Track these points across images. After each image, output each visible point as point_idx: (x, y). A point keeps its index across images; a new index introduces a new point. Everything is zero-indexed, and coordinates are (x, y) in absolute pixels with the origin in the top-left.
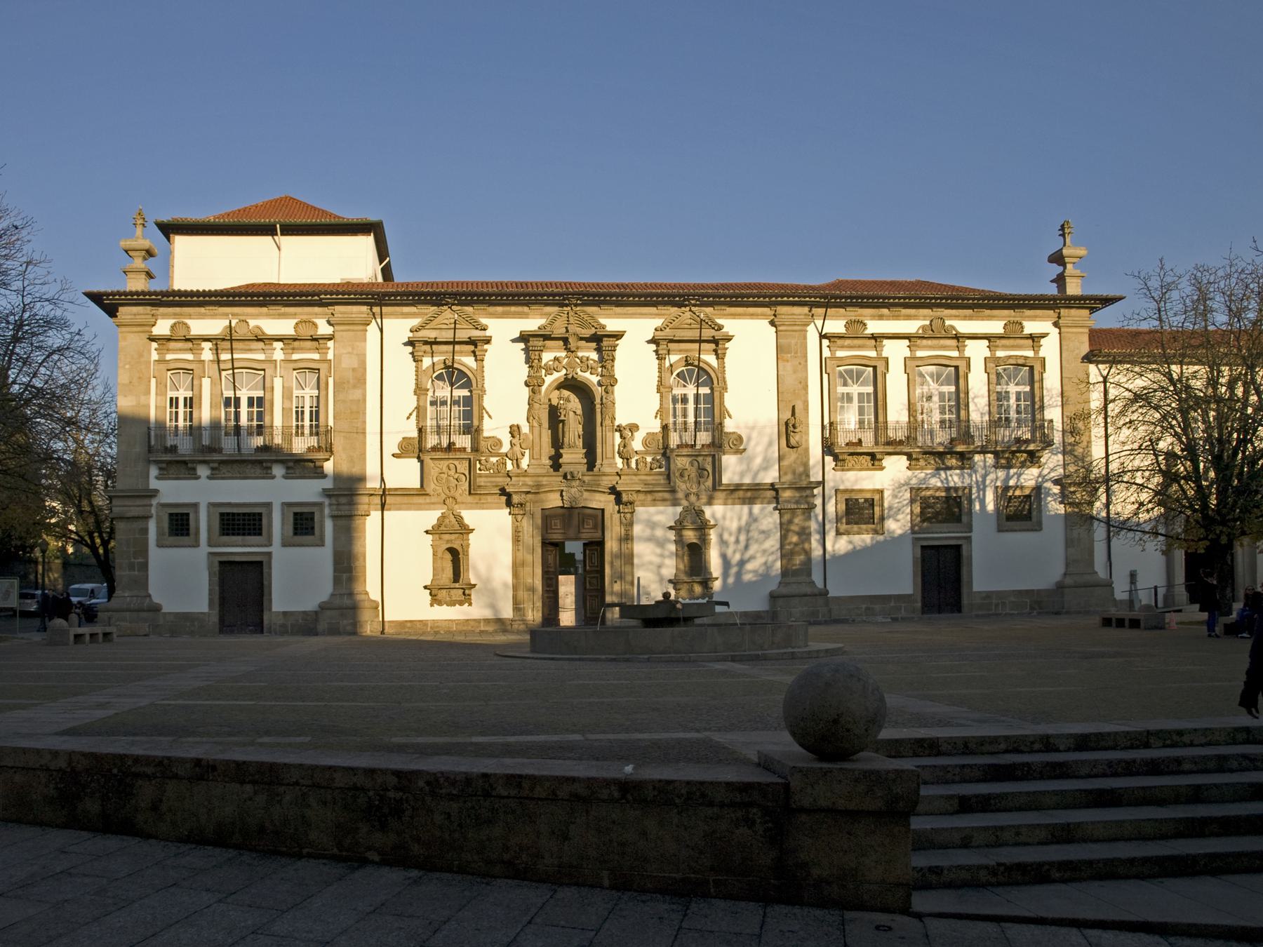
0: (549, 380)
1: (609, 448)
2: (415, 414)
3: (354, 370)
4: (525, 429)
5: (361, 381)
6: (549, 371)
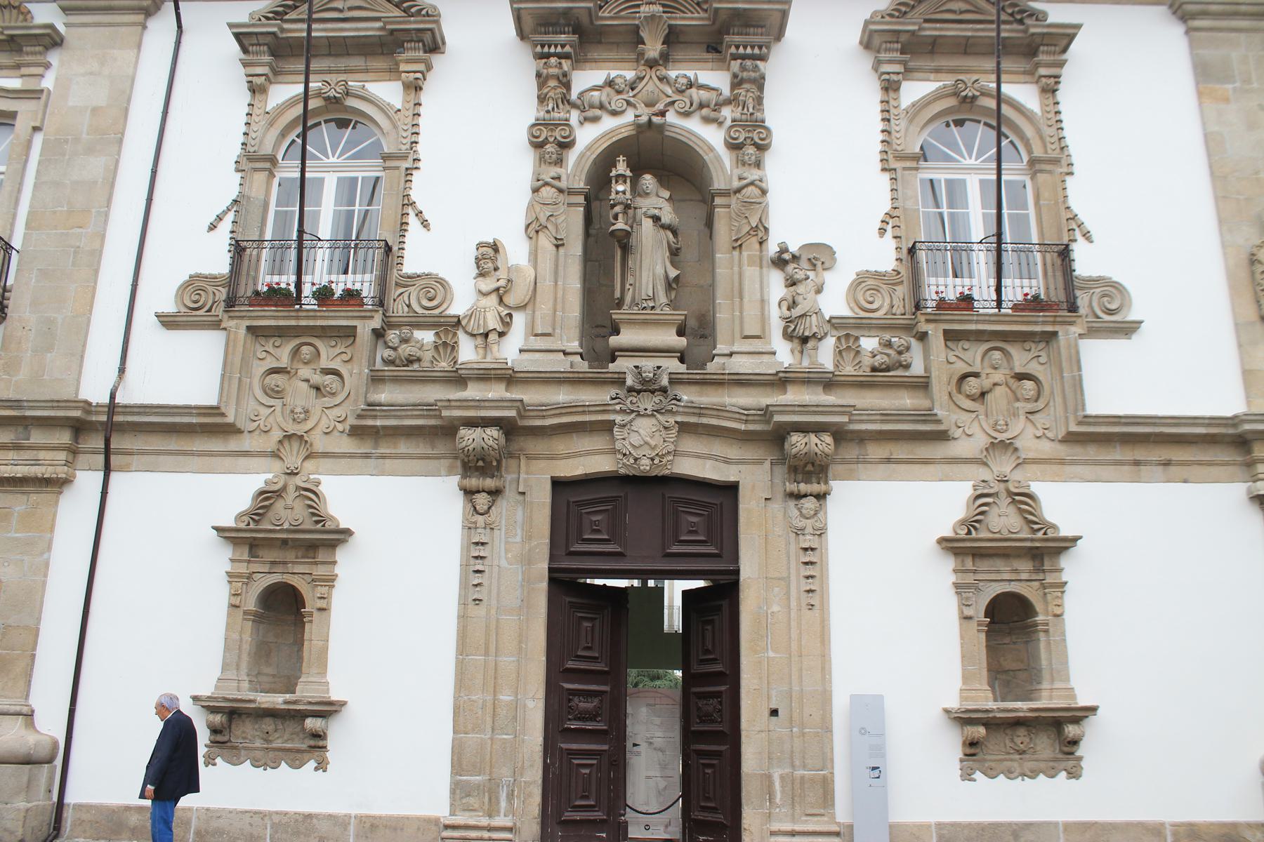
0: (589, 137)
1: (751, 310)
2: (230, 216)
3: (95, 110)
4: (517, 252)
5: (111, 136)
6: (591, 111)
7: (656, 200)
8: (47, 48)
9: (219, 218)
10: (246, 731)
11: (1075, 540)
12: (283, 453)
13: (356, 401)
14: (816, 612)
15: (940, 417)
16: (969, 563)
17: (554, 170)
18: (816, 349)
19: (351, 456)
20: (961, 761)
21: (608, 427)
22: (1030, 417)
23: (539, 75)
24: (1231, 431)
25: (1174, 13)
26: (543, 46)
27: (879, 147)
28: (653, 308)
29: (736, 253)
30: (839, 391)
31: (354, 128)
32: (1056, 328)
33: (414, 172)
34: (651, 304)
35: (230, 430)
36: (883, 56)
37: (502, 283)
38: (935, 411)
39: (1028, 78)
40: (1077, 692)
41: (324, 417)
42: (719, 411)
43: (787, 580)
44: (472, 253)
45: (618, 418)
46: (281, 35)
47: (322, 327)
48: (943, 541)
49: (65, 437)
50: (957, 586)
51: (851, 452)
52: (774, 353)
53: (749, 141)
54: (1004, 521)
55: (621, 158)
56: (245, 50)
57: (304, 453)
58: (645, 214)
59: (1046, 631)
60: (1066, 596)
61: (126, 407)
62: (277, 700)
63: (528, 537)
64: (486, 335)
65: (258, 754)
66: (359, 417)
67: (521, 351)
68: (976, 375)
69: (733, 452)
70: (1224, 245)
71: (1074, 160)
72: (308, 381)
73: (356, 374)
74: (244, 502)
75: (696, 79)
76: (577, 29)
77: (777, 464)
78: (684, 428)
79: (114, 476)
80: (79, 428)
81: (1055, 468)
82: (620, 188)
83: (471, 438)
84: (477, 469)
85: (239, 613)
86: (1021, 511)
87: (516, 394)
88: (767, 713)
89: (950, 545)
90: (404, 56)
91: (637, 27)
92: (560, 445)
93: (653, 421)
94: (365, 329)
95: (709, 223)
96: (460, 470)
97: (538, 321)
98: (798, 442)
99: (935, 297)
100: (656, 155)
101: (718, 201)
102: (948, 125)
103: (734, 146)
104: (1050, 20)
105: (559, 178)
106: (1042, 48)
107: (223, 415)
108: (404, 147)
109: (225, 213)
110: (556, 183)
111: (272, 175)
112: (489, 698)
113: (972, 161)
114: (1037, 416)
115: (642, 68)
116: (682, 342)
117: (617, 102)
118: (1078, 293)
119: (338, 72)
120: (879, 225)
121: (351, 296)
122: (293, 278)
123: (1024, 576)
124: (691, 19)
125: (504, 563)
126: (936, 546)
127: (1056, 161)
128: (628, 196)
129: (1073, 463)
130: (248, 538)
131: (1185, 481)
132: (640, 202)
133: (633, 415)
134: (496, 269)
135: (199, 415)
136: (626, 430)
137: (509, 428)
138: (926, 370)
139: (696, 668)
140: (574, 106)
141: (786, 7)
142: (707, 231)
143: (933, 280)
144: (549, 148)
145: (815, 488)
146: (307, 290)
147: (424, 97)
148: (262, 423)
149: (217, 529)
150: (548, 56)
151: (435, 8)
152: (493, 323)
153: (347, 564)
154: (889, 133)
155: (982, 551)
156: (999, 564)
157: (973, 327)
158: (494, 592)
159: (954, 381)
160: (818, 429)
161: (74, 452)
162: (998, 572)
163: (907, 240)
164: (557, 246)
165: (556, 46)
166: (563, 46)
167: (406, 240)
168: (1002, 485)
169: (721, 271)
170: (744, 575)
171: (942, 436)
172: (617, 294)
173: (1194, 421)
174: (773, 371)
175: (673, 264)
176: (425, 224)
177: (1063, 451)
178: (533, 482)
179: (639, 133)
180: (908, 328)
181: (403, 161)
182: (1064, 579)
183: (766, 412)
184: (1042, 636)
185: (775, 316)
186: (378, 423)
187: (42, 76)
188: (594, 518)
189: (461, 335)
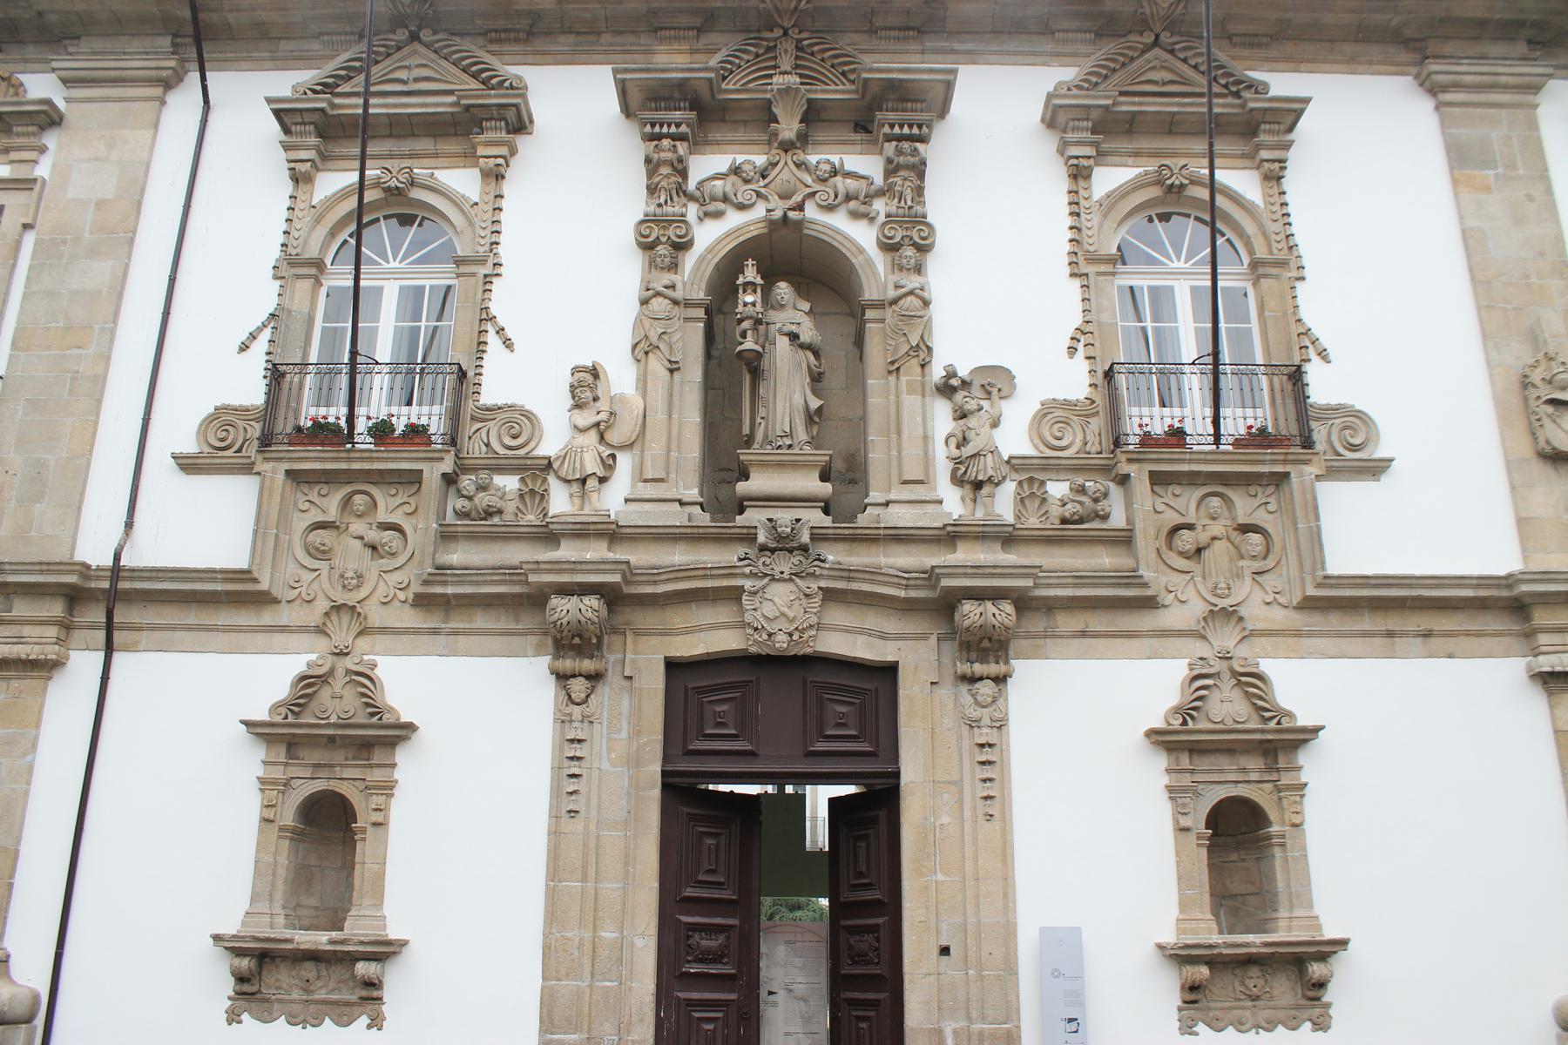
0: (710, 236)
1: (911, 450)
2: (266, 334)
3: (100, 204)
4: (621, 378)
5: (119, 235)
7: (793, 313)
8: (42, 128)
9: (253, 336)
10: (281, 980)
11: (1316, 730)
12: (330, 629)
13: (421, 563)
14: (996, 824)
15: (1146, 579)
16: (1185, 761)
17: (667, 278)
18: (991, 496)
19: (416, 632)
20: (1180, 1009)
21: (735, 595)
22: (1258, 578)
23: (648, 161)
24: (1505, 593)
25: (1421, 85)
26: (653, 125)
27: (1067, 247)
28: (790, 446)
29: (892, 378)
30: (1023, 549)
31: (420, 225)
32: (1288, 468)
33: (494, 280)
34: (788, 442)
35: (264, 599)
36: (1070, 136)
37: (603, 416)
38: (1141, 572)
39: (1247, 163)
40: (1322, 921)
41: (382, 583)
42: (873, 574)
43: (958, 783)
44: (566, 379)
45: (748, 584)
46: (330, 112)
47: (380, 471)
48: (1152, 733)
49: (56, 609)
50: (1170, 789)
51: (1037, 623)
52: (941, 502)
53: (907, 241)
54: (1228, 708)
55: (750, 262)
56: (286, 130)
57: (356, 629)
58: (780, 331)
59: (1283, 845)
60: (1306, 800)
61: (133, 570)
62: (320, 939)
63: (636, 732)
64: (583, 481)
65: (296, 1008)
66: (426, 583)
67: (627, 501)
68: (1190, 527)
69: (892, 625)
70: (1490, 365)
71: (1305, 262)
72: (362, 538)
73: (420, 530)
74: (282, 690)
75: (842, 165)
76: (696, 105)
77: (946, 639)
78: (829, 595)
79: (118, 658)
80: (74, 597)
81: (1290, 640)
82: (749, 299)
83: (565, 609)
84: (572, 647)
85: (275, 828)
86: (1248, 695)
87: (620, 554)
88: (936, 951)
89: (1161, 739)
90: (482, 138)
91: (769, 102)
92: (677, 617)
93: (791, 587)
94: (433, 473)
95: (859, 342)
96: (551, 649)
97: (648, 464)
98: (970, 612)
99: (1138, 431)
100: (793, 259)
101: (869, 314)
102: (1150, 220)
103: (889, 247)
104: (1271, 93)
105: (673, 287)
106: (1263, 127)
107: (255, 580)
108: (482, 249)
109: (260, 329)
110: (669, 292)
111: (318, 283)
112: (588, 935)
113: (1181, 264)
114: (1267, 576)
115: (774, 151)
116: (826, 489)
117: (744, 194)
118: (1313, 424)
119: (402, 157)
120: (1068, 343)
121: (416, 433)
122: (344, 411)
123: (1254, 776)
124: (834, 92)
125: (606, 765)
126: (1145, 742)
127: (1282, 264)
128: (759, 308)
129: (1311, 634)
130: (287, 734)
131: (1450, 656)
132: (773, 315)
133: (766, 580)
134: (596, 399)
135: (225, 580)
136: (757, 599)
137: (612, 597)
138: (1128, 521)
139: (847, 896)
140: (692, 198)
141: (951, 77)
142: (856, 351)
143: (1135, 411)
144: (661, 250)
145: (993, 669)
146: (361, 425)
147: (507, 188)
148: (304, 590)
149: (247, 723)
150: (659, 137)
151: (520, 79)
152: (592, 466)
153: (409, 768)
154: (1079, 230)
155: (1205, 746)
156: (1223, 761)
157: (1185, 468)
158: (594, 801)
159: (1165, 531)
160: (995, 595)
161: (67, 626)
162: (1221, 771)
163: (1103, 361)
164: (671, 371)
165: (669, 126)
166: (678, 125)
167: (484, 363)
168: (1225, 664)
169: (875, 401)
170: (905, 779)
171: (1149, 603)
172: (746, 430)
173: (1460, 581)
174: (939, 525)
175: (815, 393)
176: (508, 344)
177: (1298, 620)
178: (642, 664)
179: (771, 231)
180: (1105, 470)
181: (480, 266)
182: (1303, 780)
183: (932, 575)
184: (1277, 851)
185: (941, 455)
186: (450, 590)
187: (35, 162)
188: (719, 708)
189: (553, 481)
